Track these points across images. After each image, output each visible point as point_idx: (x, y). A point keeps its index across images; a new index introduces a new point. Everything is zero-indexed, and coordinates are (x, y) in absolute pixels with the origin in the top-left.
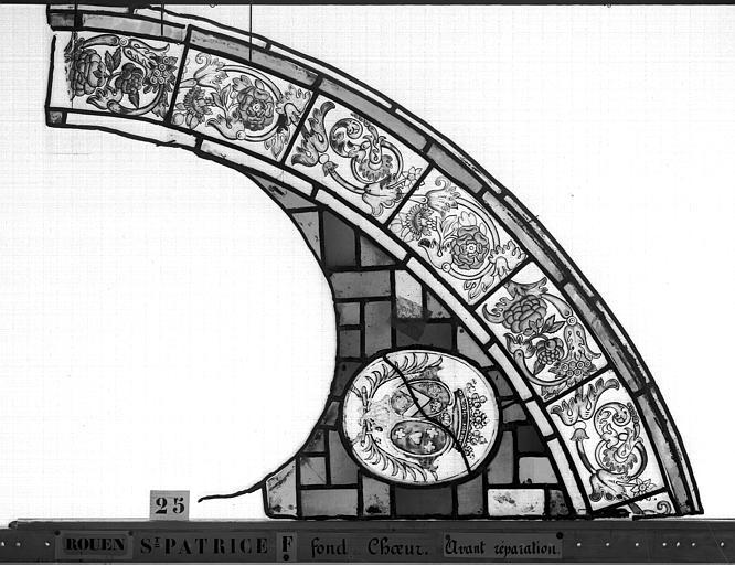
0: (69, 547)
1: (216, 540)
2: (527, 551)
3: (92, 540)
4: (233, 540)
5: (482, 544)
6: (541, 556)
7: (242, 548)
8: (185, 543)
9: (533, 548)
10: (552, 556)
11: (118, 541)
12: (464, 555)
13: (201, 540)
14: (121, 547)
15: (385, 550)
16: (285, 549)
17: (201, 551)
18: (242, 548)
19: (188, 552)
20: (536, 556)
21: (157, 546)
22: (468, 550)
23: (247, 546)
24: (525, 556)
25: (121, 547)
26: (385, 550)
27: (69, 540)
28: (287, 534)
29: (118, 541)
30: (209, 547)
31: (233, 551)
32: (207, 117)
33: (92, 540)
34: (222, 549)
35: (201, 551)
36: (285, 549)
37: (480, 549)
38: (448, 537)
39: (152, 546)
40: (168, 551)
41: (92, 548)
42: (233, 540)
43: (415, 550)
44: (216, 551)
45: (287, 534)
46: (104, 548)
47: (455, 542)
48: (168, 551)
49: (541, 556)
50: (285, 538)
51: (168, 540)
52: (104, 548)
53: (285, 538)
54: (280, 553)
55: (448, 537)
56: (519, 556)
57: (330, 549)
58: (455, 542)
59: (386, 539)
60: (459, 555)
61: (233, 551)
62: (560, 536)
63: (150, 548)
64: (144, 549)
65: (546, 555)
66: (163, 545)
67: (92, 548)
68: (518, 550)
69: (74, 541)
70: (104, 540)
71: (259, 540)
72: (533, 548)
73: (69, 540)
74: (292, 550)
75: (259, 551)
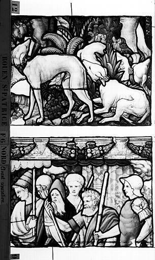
2: (2, 193)
7: (4, 117)
11: (7, 77)
17: (3, 104)
18: (4, 117)
19: (3, 100)
29: (7, 77)
30: (4, 107)
34: (3, 111)
35: (3, 104)
39: (5, 88)
40: (3, 93)
48: (3, 93)
63: (4, 87)
66: (4, 92)
69: (6, 65)
71: (6, 123)
75: (3, 123)
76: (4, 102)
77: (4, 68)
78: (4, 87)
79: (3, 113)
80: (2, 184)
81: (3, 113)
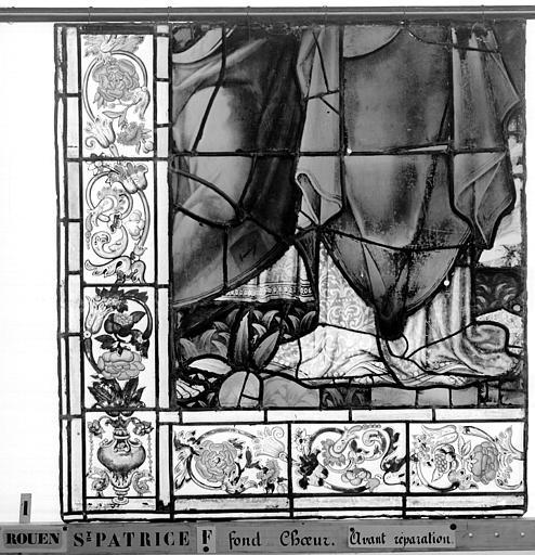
0: (9, 542)
1: (142, 534)
2: (424, 541)
3: (30, 535)
4: (158, 534)
5: (383, 536)
6: (436, 545)
8: (114, 537)
9: (428, 539)
10: (446, 546)
11: (53, 535)
12: (367, 546)
13: (129, 535)
14: (57, 541)
15: (296, 542)
16: (205, 542)
17: (129, 544)
19: (117, 545)
20: (433, 545)
21: (89, 539)
22: (370, 540)
23: (170, 539)
24: (421, 546)
25: (57, 541)
26: (296, 542)
27: (9, 535)
28: (207, 528)
29: (53, 535)
30: (136, 540)
31: (158, 544)
32: (139, 122)
33: (30, 535)
34: (148, 544)
35: (129, 544)
36: (205, 542)
37: (380, 540)
38: (352, 529)
40: (98, 545)
41: (30, 542)
42: (158, 534)
43: (322, 542)
44: (142, 545)
45: (207, 528)
46: (41, 542)
47: (358, 534)
48: (98, 545)
49: (436, 545)
50: (205, 532)
51: (98, 535)
52: (41, 542)
53: (205, 532)
54: (201, 546)
55: (352, 529)
56: (416, 546)
57: (317, 542)
58: (358, 534)
59: (297, 532)
60: (365, 546)
61: (158, 544)
62: (453, 527)
63: (82, 542)
64: (78, 543)
65: (441, 545)
66: (94, 539)
67: (30, 542)
68: (416, 540)
69: (14, 536)
70: (41, 535)
71: (181, 534)
72: (428, 539)
73: (9, 535)
74: (211, 543)
75: (181, 544)
76: (122, 540)
77: (33, 541)
78: (82, 542)
79: (153, 539)
80: (398, 540)
81: (153, 539)
